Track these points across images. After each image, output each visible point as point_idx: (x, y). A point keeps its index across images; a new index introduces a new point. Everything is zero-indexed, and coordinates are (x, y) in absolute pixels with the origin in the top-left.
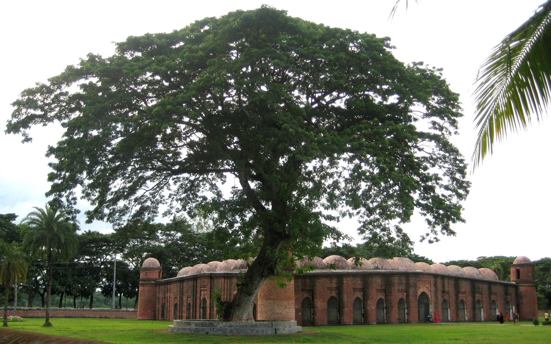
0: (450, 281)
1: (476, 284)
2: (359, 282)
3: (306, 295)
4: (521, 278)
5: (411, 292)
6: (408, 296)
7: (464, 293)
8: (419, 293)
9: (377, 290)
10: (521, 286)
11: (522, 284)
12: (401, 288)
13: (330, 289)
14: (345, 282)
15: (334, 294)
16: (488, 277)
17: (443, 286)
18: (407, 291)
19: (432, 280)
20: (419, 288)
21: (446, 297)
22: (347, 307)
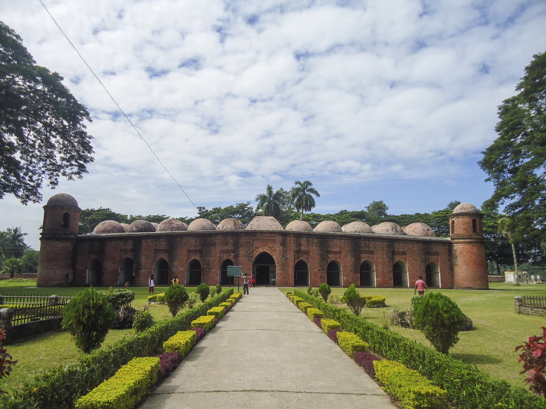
0: (311, 240)
1: (362, 242)
2: (164, 243)
3: (94, 257)
4: (455, 233)
5: (242, 252)
6: (236, 257)
7: (339, 252)
8: (256, 254)
9: (189, 251)
10: (456, 243)
12: (225, 248)
14: (144, 244)
15: (129, 255)
16: (413, 234)
17: (299, 245)
18: (235, 251)
19: (279, 239)
21: (303, 258)
22: (145, 269)
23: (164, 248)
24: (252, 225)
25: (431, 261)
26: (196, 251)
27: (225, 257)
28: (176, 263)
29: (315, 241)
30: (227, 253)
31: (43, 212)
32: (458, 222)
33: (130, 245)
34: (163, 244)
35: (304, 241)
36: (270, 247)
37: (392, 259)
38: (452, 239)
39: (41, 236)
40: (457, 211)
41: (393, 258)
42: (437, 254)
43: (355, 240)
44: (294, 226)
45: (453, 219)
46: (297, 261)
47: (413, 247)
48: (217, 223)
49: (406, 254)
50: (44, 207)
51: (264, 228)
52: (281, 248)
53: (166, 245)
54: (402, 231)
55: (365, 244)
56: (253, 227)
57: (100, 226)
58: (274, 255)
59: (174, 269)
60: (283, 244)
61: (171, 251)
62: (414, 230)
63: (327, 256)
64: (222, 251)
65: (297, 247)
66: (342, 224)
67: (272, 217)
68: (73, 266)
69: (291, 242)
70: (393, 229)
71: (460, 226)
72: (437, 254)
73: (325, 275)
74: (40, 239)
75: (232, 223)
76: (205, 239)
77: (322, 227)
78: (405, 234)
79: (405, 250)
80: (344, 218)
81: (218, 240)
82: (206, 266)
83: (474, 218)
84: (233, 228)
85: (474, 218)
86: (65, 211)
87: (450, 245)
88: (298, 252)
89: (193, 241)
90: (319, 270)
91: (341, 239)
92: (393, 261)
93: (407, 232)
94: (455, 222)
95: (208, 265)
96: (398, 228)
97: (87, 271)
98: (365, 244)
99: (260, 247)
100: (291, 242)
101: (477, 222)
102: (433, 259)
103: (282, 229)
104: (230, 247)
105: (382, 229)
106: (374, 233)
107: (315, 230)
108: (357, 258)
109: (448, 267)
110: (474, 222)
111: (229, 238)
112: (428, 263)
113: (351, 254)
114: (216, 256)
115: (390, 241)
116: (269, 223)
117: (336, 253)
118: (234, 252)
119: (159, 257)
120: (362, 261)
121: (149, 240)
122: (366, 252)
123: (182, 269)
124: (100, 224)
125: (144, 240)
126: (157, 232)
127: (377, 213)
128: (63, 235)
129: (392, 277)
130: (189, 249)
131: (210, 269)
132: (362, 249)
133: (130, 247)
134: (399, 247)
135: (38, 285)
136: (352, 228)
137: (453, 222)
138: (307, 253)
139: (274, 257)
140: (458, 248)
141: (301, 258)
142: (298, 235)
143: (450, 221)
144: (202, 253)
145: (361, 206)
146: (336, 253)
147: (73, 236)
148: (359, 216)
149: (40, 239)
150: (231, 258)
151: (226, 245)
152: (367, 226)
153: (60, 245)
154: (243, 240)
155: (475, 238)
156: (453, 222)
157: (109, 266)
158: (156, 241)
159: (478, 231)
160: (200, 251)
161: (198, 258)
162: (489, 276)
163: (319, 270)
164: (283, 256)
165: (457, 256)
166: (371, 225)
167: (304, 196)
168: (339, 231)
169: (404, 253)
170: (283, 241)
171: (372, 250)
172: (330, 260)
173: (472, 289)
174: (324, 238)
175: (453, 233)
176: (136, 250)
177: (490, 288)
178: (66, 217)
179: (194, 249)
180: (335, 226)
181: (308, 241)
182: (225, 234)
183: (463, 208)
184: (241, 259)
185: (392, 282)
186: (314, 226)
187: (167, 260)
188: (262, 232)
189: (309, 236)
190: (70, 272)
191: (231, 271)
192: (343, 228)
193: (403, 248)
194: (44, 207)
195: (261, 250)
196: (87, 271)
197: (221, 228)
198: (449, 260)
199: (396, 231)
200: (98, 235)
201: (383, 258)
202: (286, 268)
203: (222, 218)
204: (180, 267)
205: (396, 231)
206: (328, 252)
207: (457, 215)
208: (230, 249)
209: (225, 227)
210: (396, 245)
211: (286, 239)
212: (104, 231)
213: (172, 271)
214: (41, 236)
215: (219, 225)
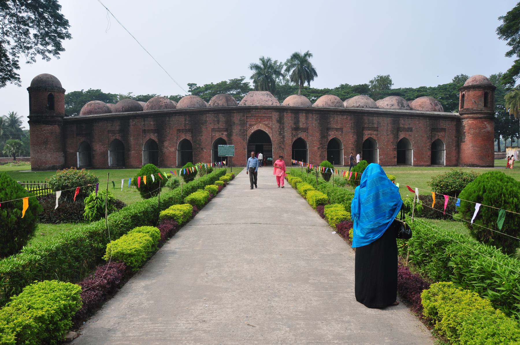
2: (152, 123)
3: (82, 139)
5: (236, 130)
6: (229, 135)
7: (341, 129)
9: (179, 131)
10: (464, 118)
11: (465, 116)
13: (113, 132)
14: (131, 124)
15: (118, 137)
17: (297, 122)
19: (275, 115)
20: (251, 125)
21: (302, 135)
22: (134, 150)
23: (152, 128)
24: (246, 101)
25: (437, 138)
26: (186, 131)
27: (217, 135)
28: (166, 144)
29: (315, 117)
30: (220, 131)
31: (27, 94)
32: (468, 95)
33: (117, 126)
34: (151, 123)
35: (302, 118)
36: (266, 125)
37: (396, 136)
38: (461, 114)
39: (28, 119)
40: (468, 83)
41: (398, 135)
42: (444, 130)
43: (358, 116)
44: (291, 101)
45: (464, 92)
46: (295, 139)
47: (419, 123)
48: (208, 101)
49: (411, 131)
50: (29, 89)
51: (259, 103)
52: (278, 125)
53: (154, 125)
54: (408, 106)
55: (369, 119)
56: (246, 103)
57: (85, 108)
59: (165, 150)
60: (280, 121)
61: (160, 130)
62: (422, 105)
63: (327, 133)
64: (213, 130)
65: (295, 124)
66: (343, 100)
67: (267, 92)
68: (64, 149)
69: (288, 119)
70: (398, 103)
71: (471, 100)
72: (444, 130)
73: (325, 154)
74: (29, 122)
75: (224, 100)
76: (194, 117)
77: (321, 102)
78: (411, 109)
79: (411, 126)
80: (345, 91)
81: (209, 118)
82: (198, 146)
83: (486, 91)
84: (225, 105)
85: (486, 91)
86: (49, 93)
87: (458, 121)
88: (297, 129)
89: (182, 119)
90: (319, 148)
91: (343, 115)
92: (398, 138)
93: (413, 107)
94: (466, 95)
95: (200, 145)
96: (405, 102)
97: (78, 153)
98: (369, 119)
99: (254, 125)
100: (288, 119)
101: (489, 96)
102: (440, 135)
103: (278, 105)
104: (222, 125)
105: (386, 104)
106: (378, 108)
107: (315, 105)
108: (359, 133)
109: (455, 144)
110: (486, 96)
111: (221, 116)
112: (433, 140)
114: (208, 135)
115: (395, 117)
116: (265, 98)
117: (337, 130)
118: (227, 130)
119: (147, 138)
120: (365, 138)
121: (136, 120)
122: (370, 129)
123: (173, 149)
124: (86, 106)
125: (131, 121)
126: (144, 111)
127: (382, 87)
128: (49, 118)
129: (396, 155)
130: (179, 128)
131: (202, 149)
132: (366, 126)
133: (118, 128)
134: (404, 123)
135: (33, 169)
136: (355, 102)
137: (463, 96)
138: (305, 130)
139: (270, 135)
140: (467, 123)
141: (299, 136)
142: (295, 111)
143: (460, 94)
144: (192, 133)
145: (364, 78)
146: (337, 130)
147: (60, 118)
148: (361, 90)
149: (29, 122)
150: (224, 137)
151: (218, 123)
152: (371, 101)
153: (48, 128)
154: (236, 118)
155: (486, 113)
156: (463, 96)
157: (98, 148)
158: (144, 121)
159: (489, 105)
160: (191, 131)
161: (188, 137)
162: (495, 153)
163: (319, 148)
164: (280, 134)
165: (465, 132)
166: (375, 99)
167: (303, 68)
168: (341, 106)
169: (410, 130)
171: (375, 126)
172: (330, 138)
173: (477, 166)
174: (324, 114)
175: (462, 107)
176: (124, 131)
177: (495, 165)
178: (51, 99)
179: (184, 128)
180: (336, 101)
181: (307, 118)
182: (216, 111)
183: (475, 80)
184: (234, 137)
185: (396, 160)
186: (314, 101)
187: (156, 140)
188: (256, 108)
189: (309, 111)
190: (61, 154)
191: (223, 150)
192: (345, 104)
193: (410, 124)
194: (29, 89)
195: (255, 128)
196: (78, 153)
197: (212, 105)
198: (456, 137)
199: (403, 106)
200: (84, 116)
201: (388, 135)
202: (283, 147)
203: (213, 94)
204: (170, 147)
205: (403, 106)
206: (328, 129)
207: (469, 88)
208: (222, 127)
209: (216, 104)
210: (402, 121)
211: (283, 115)
212: (90, 112)
213: (162, 152)
214: (28, 119)
215: (210, 101)
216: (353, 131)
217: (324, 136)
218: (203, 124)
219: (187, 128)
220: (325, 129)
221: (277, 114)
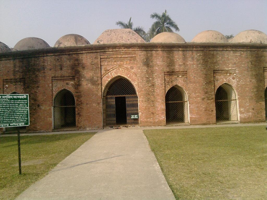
0: (189, 54)
8: (106, 80)
17: (171, 63)
20: (107, 71)
21: (180, 82)
26: (16, 81)
29: (197, 55)
58: (134, 80)
60: (148, 63)
69: (159, 60)
88: (171, 73)
113: (250, 73)
139: (135, 84)
164: (148, 81)
170: (147, 59)
181: (185, 58)
188: (114, 47)
195: (113, 74)
211: (152, 55)
216: (250, 73)
217: (209, 81)
218: (39, 70)
219: (18, 77)
220: (211, 71)
221: (144, 53)
